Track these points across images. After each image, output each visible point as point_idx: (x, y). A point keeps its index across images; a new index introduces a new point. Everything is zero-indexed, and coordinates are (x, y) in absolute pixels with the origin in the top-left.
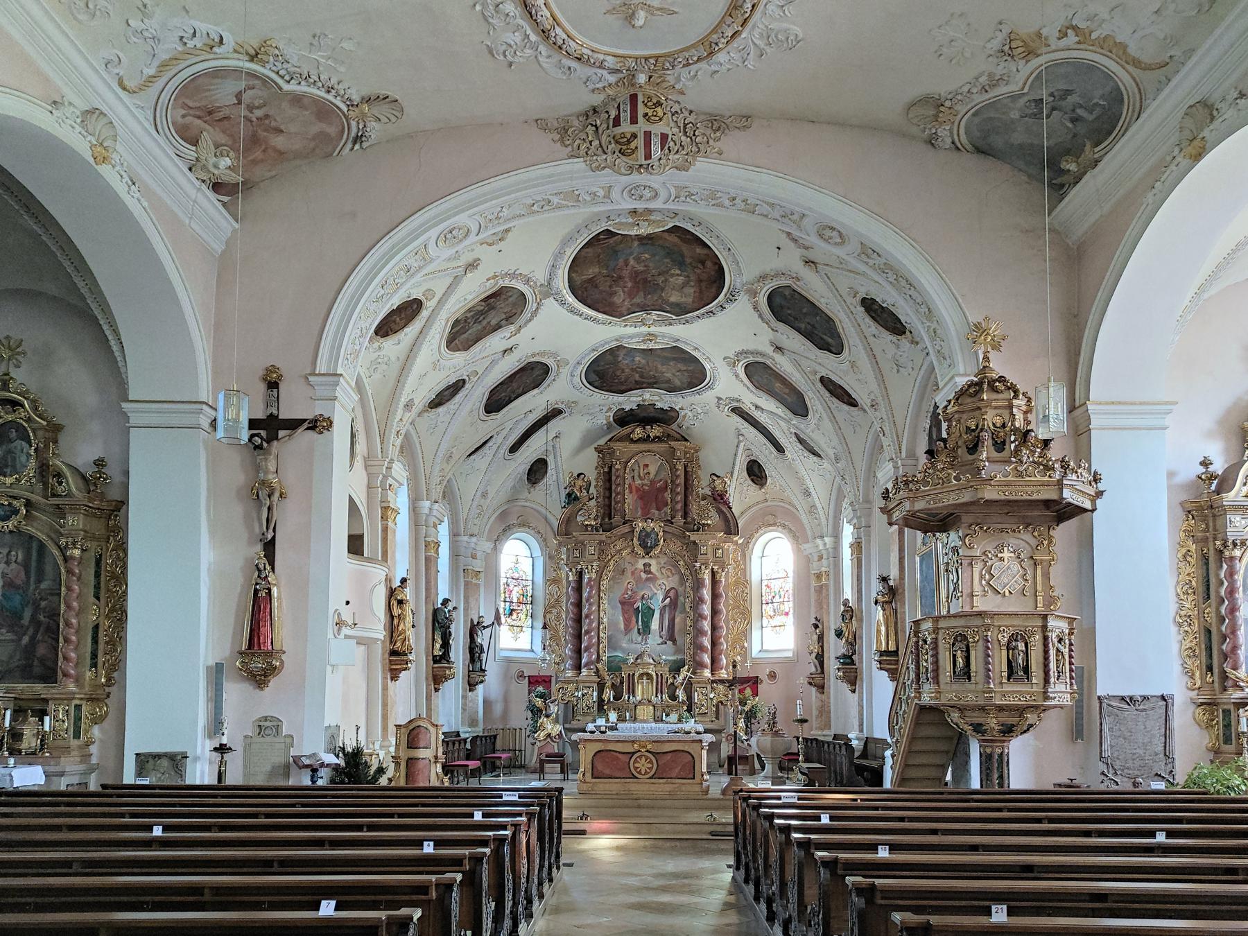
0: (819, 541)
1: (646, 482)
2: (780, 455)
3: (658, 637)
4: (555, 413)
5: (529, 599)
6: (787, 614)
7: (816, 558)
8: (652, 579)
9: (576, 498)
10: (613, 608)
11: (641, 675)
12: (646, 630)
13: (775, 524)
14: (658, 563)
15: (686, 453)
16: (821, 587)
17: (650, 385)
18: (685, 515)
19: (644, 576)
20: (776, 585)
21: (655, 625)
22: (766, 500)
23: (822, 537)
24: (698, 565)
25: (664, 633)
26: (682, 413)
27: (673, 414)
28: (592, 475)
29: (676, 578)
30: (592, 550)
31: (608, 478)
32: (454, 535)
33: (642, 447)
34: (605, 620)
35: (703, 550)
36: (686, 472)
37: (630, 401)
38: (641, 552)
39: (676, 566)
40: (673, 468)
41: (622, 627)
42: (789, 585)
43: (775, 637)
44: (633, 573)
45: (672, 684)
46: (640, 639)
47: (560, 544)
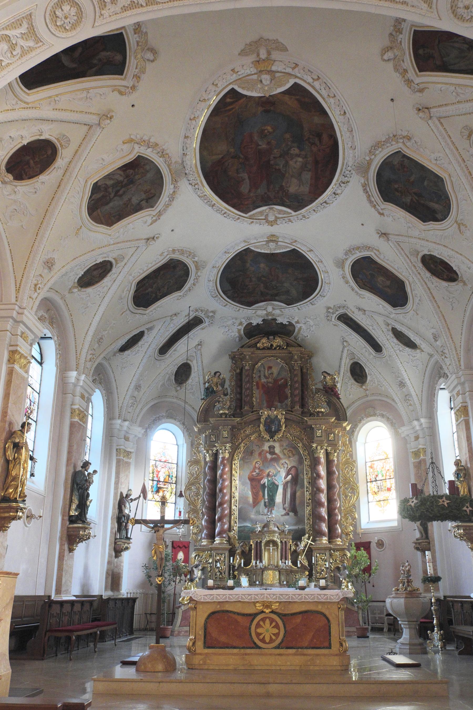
0: (416, 423)
1: (270, 380)
2: (377, 355)
3: (281, 509)
4: (194, 323)
5: (174, 479)
6: (389, 489)
7: (413, 439)
8: (276, 459)
9: (213, 392)
10: (243, 484)
11: (268, 543)
12: (271, 504)
13: (375, 415)
14: (281, 446)
15: (301, 358)
16: (420, 462)
17: (273, 298)
18: (303, 406)
19: (269, 456)
20: (378, 466)
21: (279, 498)
22: (367, 396)
23: (418, 420)
24: (314, 445)
25: (287, 505)
26: (298, 326)
28: (226, 375)
29: (297, 457)
30: (225, 434)
31: (240, 376)
32: (110, 416)
33: (267, 352)
34: (237, 495)
35: (319, 433)
37: (257, 314)
38: (267, 436)
39: (296, 448)
40: (291, 369)
41: (251, 500)
42: (390, 465)
43: (378, 510)
44: (260, 454)
45: (295, 551)
46: (266, 511)
47: (201, 431)
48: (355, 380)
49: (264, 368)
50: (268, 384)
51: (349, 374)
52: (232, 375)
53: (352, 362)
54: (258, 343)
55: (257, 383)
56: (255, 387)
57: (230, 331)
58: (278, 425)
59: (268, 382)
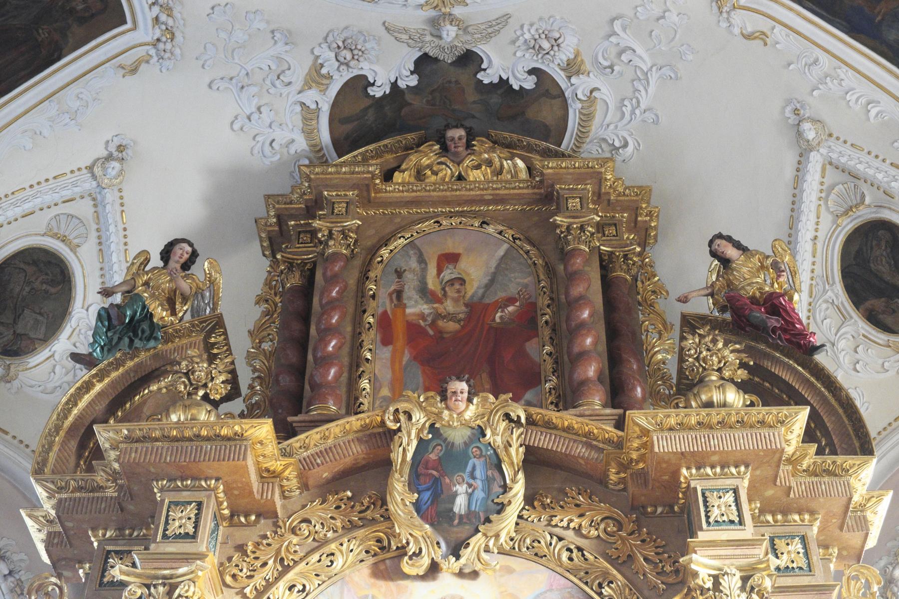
1: (449, 306)
26: (577, 88)
27: (545, 113)
36: (607, 283)
48: (872, 318)
49: (422, 260)
50: (441, 323)
51: (838, 292)
52: (267, 313)
53: (848, 226)
54: (397, 168)
55: (385, 323)
56: (370, 338)
57: (267, 116)
58: (489, 481)
59: (438, 316)
